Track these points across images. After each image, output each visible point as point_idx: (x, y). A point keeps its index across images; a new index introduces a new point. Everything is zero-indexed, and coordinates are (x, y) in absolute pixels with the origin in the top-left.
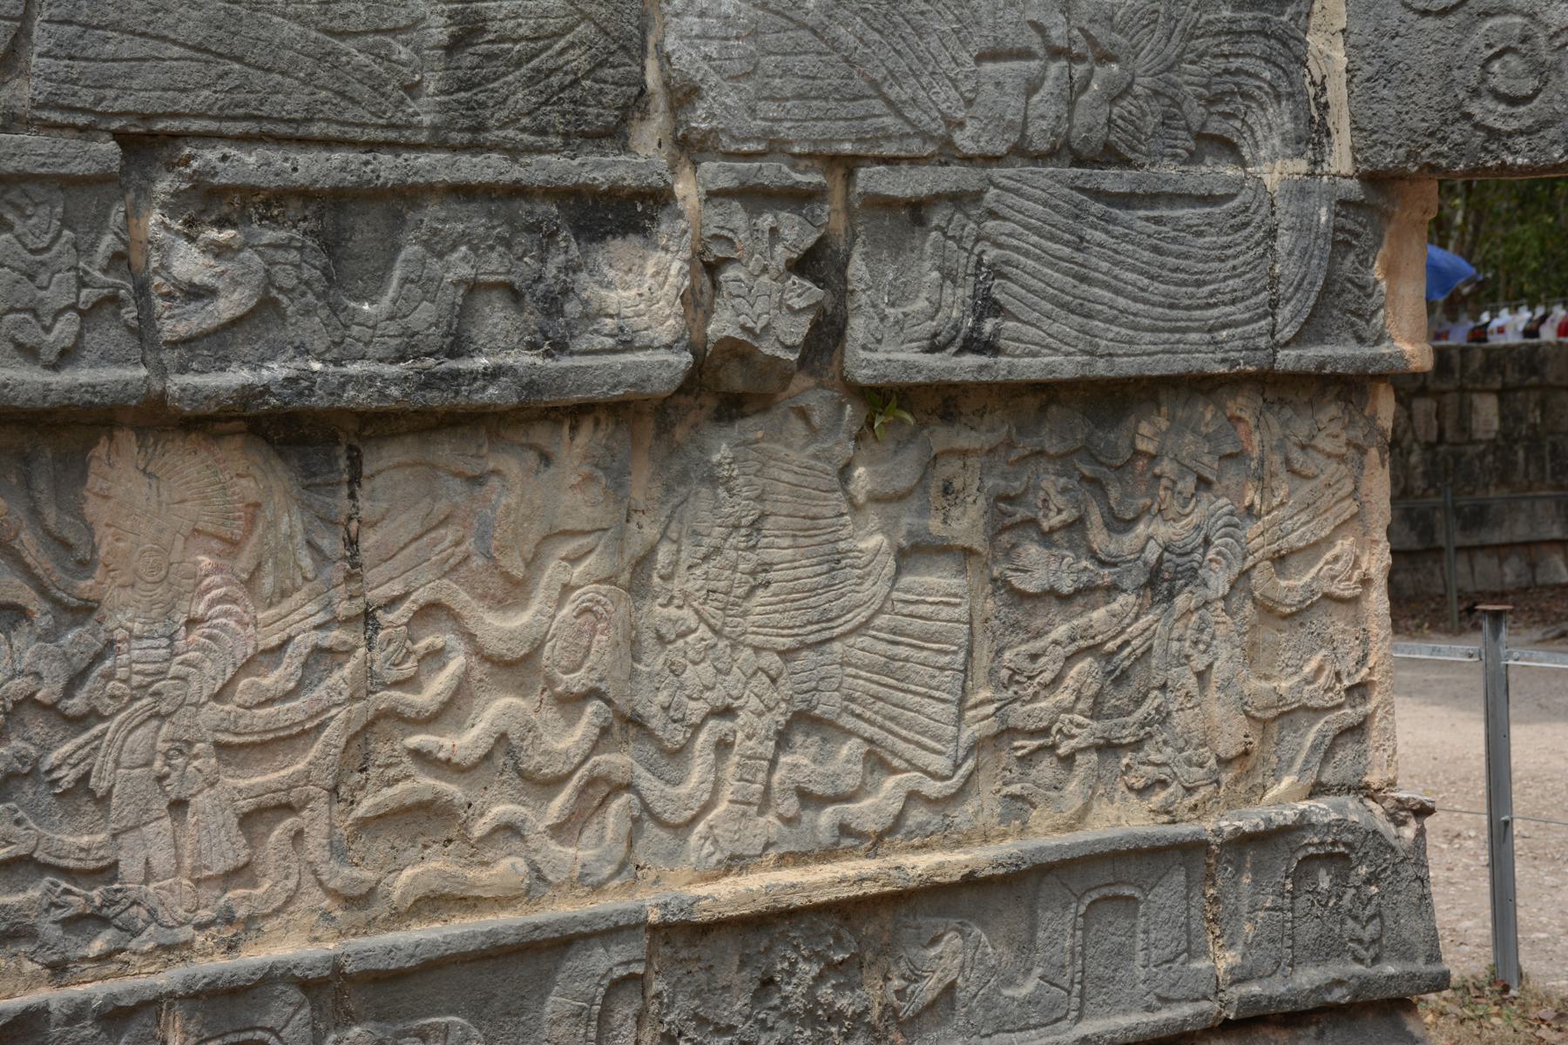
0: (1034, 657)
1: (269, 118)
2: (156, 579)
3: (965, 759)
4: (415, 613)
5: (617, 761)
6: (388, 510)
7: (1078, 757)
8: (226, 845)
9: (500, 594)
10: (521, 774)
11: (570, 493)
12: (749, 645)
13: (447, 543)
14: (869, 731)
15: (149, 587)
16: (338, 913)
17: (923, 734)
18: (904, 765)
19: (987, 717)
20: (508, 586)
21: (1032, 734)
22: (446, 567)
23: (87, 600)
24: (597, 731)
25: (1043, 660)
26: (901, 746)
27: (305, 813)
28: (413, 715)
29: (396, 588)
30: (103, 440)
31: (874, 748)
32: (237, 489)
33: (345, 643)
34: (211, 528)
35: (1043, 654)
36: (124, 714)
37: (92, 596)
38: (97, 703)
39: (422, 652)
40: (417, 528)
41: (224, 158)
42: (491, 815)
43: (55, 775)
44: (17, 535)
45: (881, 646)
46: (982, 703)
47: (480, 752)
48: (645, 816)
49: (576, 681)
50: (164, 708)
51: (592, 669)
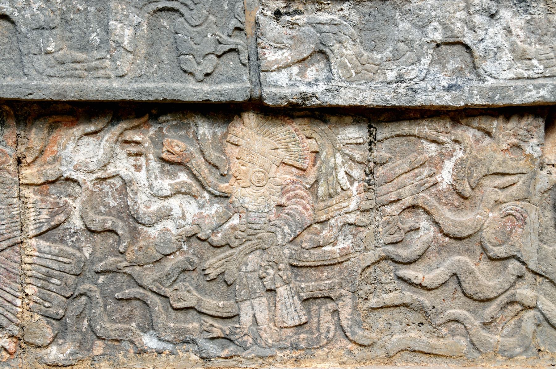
2: (261, 185)
4: (404, 210)
6: (390, 158)
8: (294, 313)
9: (457, 204)
10: (465, 294)
11: (502, 153)
13: (423, 176)
15: (258, 188)
16: (357, 352)
20: (461, 200)
22: (423, 188)
23: (224, 193)
24: (514, 277)
27: (340, 303)
28: (400, 260)
29: (393, 197)
30: (235, 118)
32: (305, 145)
33: (362, 222)
34: (290, 162)
36: (243, 246)
37: (227, 191)
38: (228, 241)
39: (407, 229)
40: (407, 167)
43: (206, 272)
44: (190, 161)
47: (440, 282)
48: (545, 324)
49: (501, 251)
50: (262, 245)
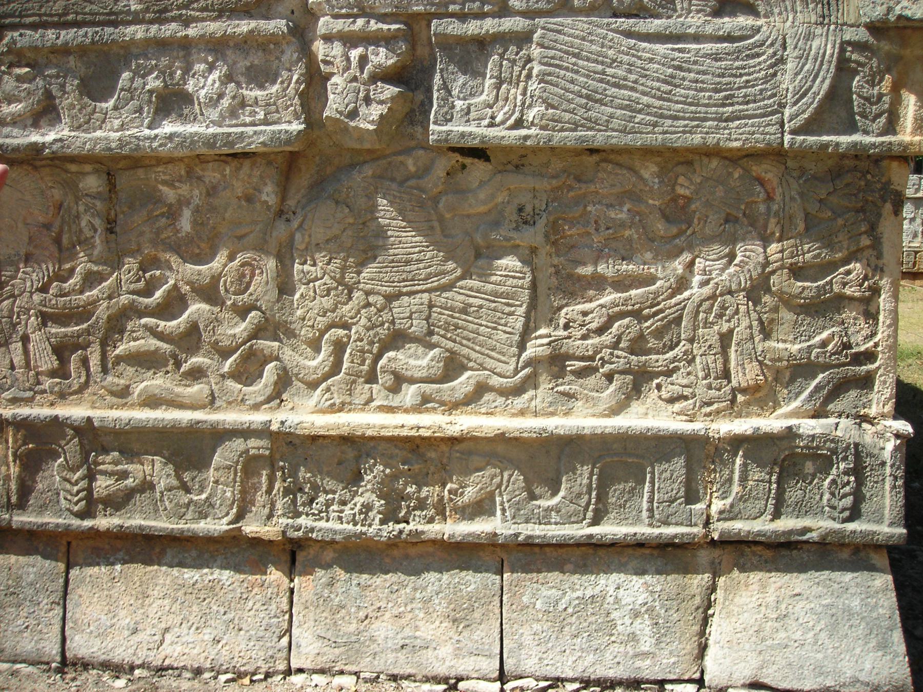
0: (585, 314)
1: (45, 15)
3: (523, 368)
5: (267, 345)
7: (616, 376)
12: (361, 290)
14: (450, 344)
17: (492, 350)
18: (477, 366)
19: (543, 345)
21: (582, 359)
25: (591, 316)
26: (474, 355)
31: (453, 356)
35: (592, 312)
41: (21, 35)
42: (189, 362)
45: (462, 298)
46: (541, 337)
51: (251, 294)
